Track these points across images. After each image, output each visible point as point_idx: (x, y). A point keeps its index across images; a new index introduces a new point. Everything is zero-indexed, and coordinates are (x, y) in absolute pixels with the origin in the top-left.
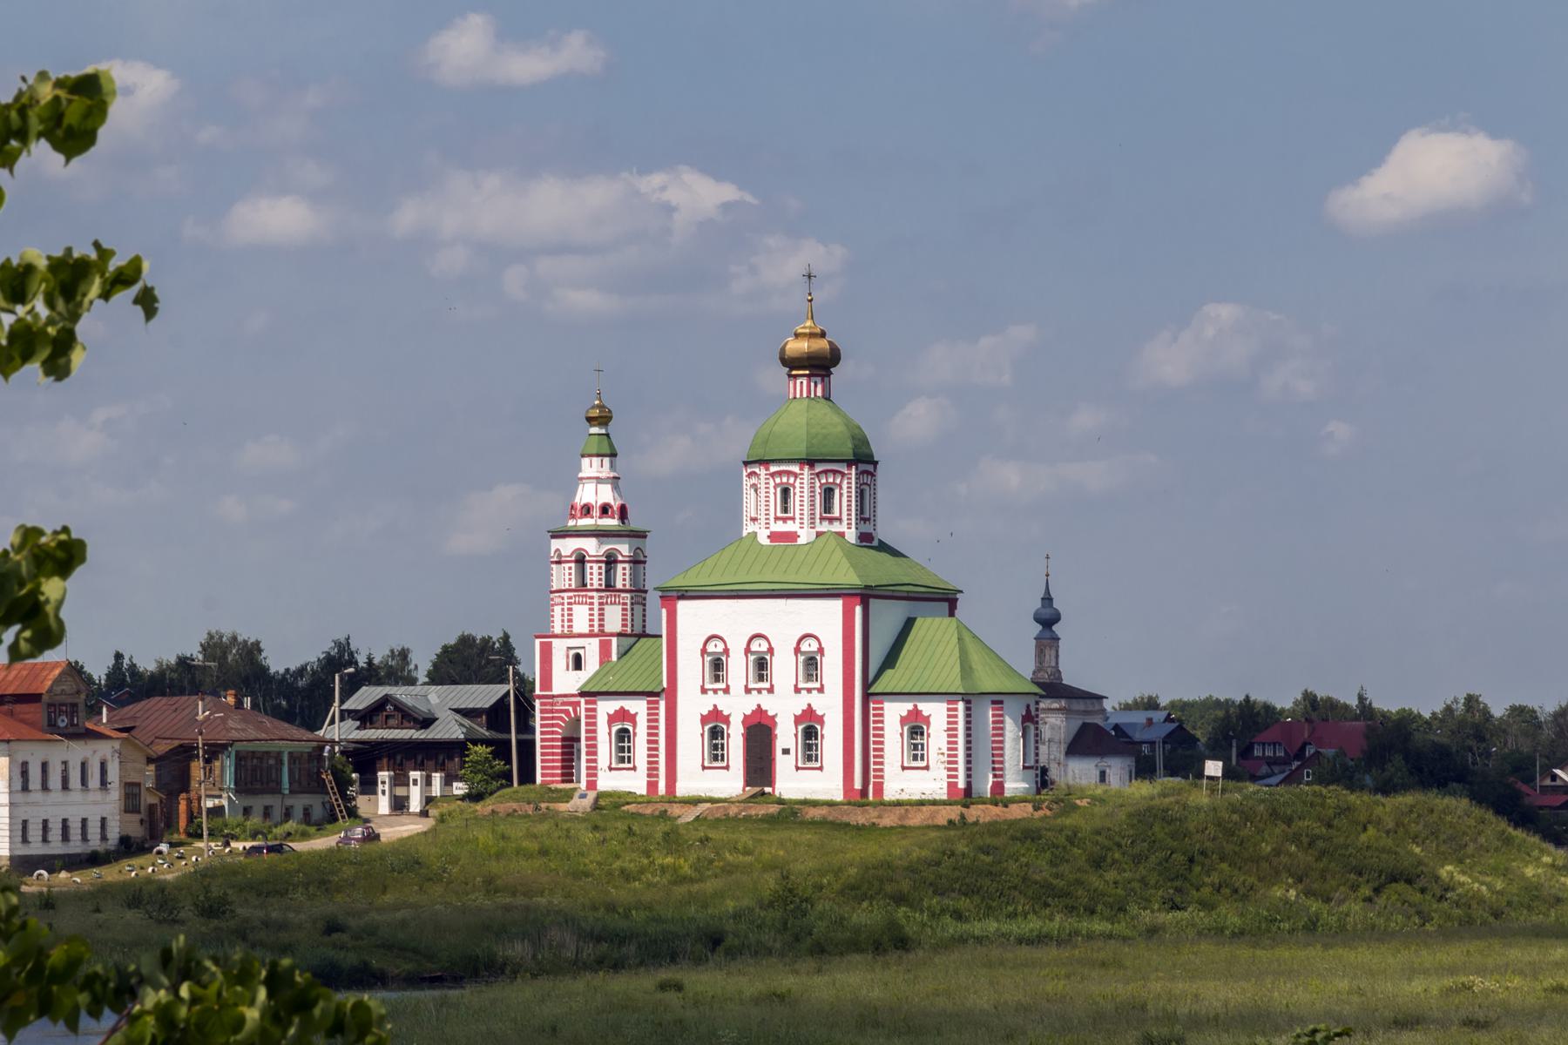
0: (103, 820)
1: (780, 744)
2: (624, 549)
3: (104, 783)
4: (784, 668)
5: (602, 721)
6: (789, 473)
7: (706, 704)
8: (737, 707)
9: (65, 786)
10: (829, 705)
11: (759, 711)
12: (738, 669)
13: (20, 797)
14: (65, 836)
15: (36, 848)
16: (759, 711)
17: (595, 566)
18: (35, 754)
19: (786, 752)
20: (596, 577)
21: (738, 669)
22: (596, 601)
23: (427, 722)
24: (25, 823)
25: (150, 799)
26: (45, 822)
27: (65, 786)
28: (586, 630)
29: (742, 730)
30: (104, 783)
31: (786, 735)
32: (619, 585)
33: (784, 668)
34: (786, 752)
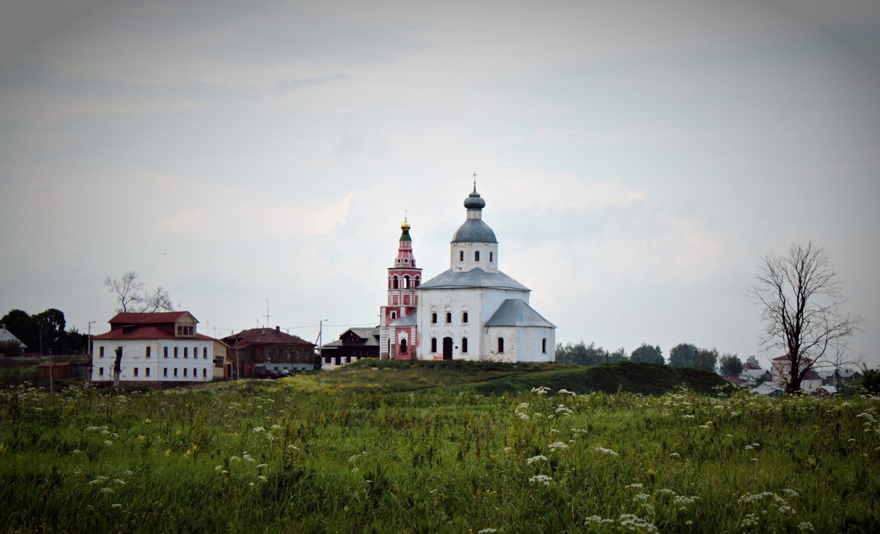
0: (205, 370)
1: (454, 346)
3: (205, 356)
4: (457, 318)
8: (441, 331)
9: (186, 355)
12: (442, 318)
13: (163, 360)
14: (185, 374)
15: (171, 378)
18: (171, 344)
21: (442, 318)
23: (366, 340)
24: (165, 370)
25: (226, 362)
26: (195, 370)
27: (186, 355)
30: (205, 356)
31: (457, 343)
33: (457, 318)
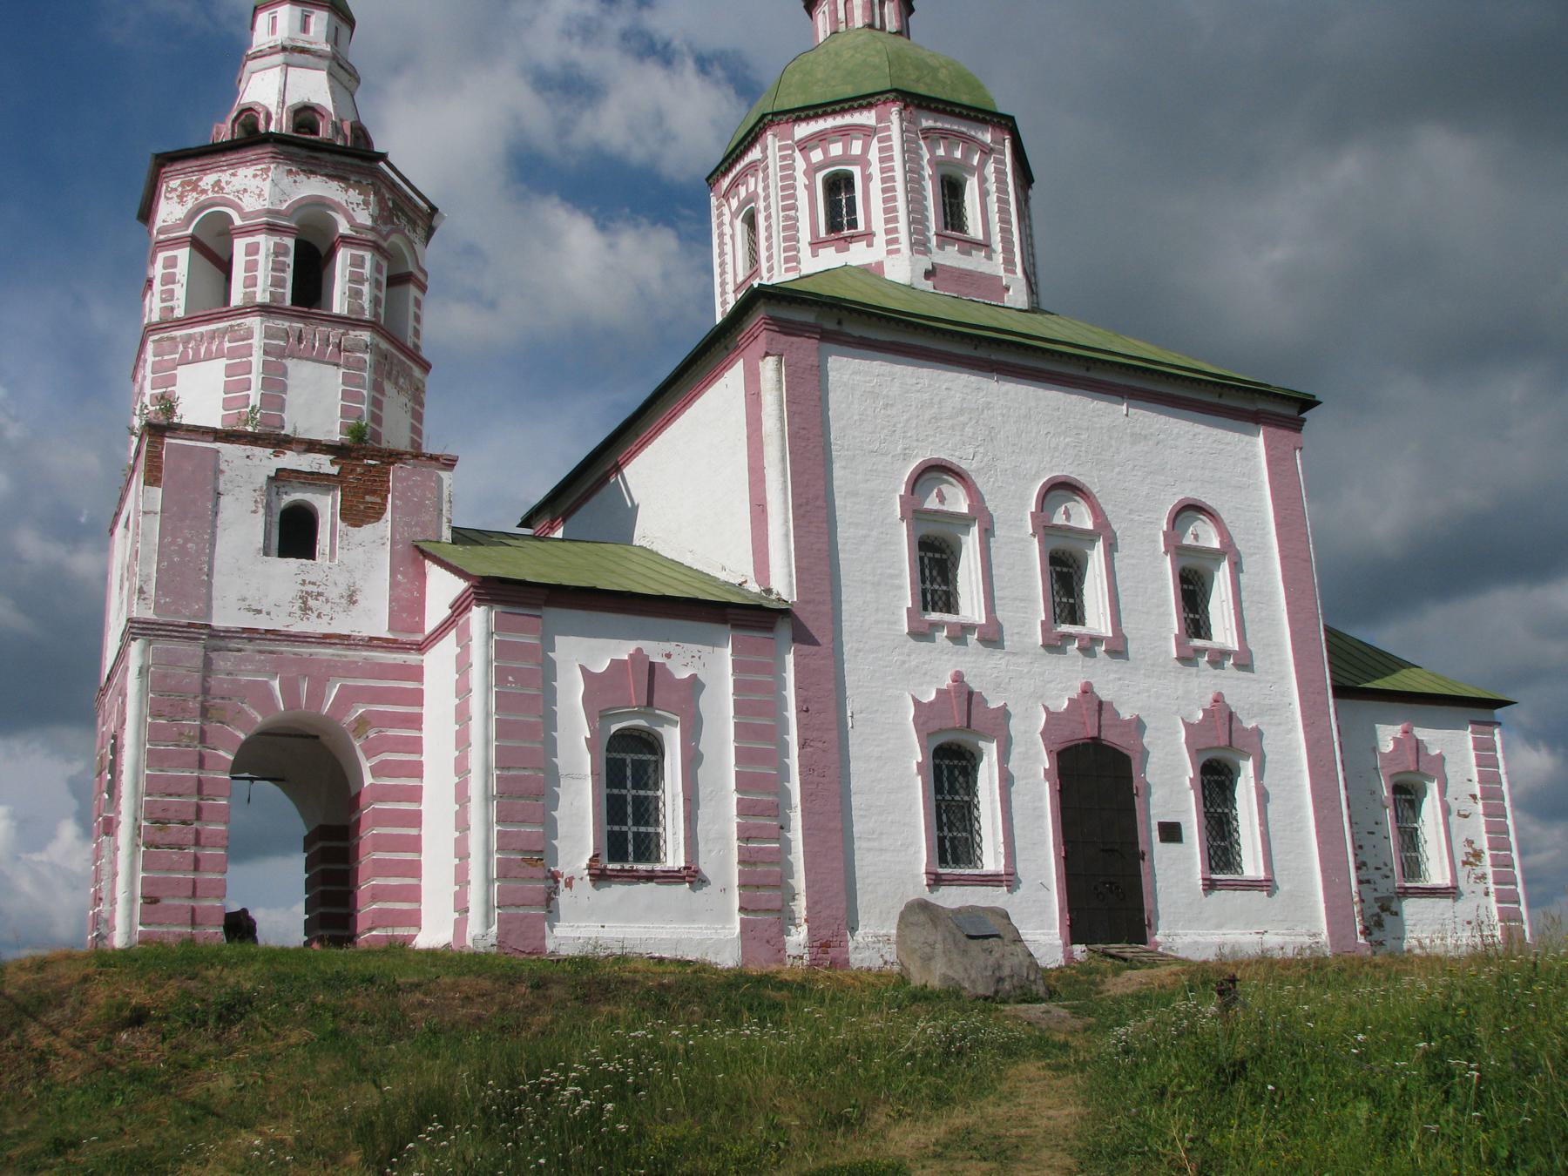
2: (351, 208)
5: (571, 694)
6: (845, 133)
7: (937, 668)
10: (1279, 700)
11: (1091, 702)
16: (1091, 702)
17: (265, 242)
19: (1171, 832)
20: (263, 274)
22: (257, 342)
28: (213, 418)
29: (1045, 762)
31: (1169, 790)
32: (339, 304)
34: (1171, 832)
